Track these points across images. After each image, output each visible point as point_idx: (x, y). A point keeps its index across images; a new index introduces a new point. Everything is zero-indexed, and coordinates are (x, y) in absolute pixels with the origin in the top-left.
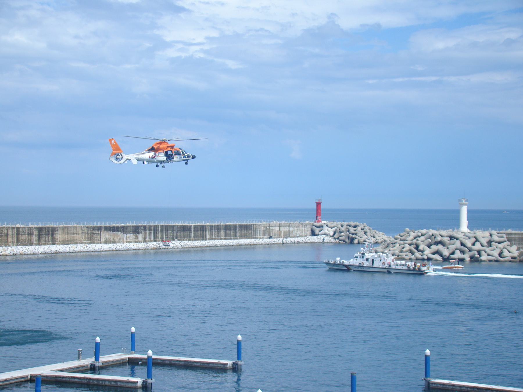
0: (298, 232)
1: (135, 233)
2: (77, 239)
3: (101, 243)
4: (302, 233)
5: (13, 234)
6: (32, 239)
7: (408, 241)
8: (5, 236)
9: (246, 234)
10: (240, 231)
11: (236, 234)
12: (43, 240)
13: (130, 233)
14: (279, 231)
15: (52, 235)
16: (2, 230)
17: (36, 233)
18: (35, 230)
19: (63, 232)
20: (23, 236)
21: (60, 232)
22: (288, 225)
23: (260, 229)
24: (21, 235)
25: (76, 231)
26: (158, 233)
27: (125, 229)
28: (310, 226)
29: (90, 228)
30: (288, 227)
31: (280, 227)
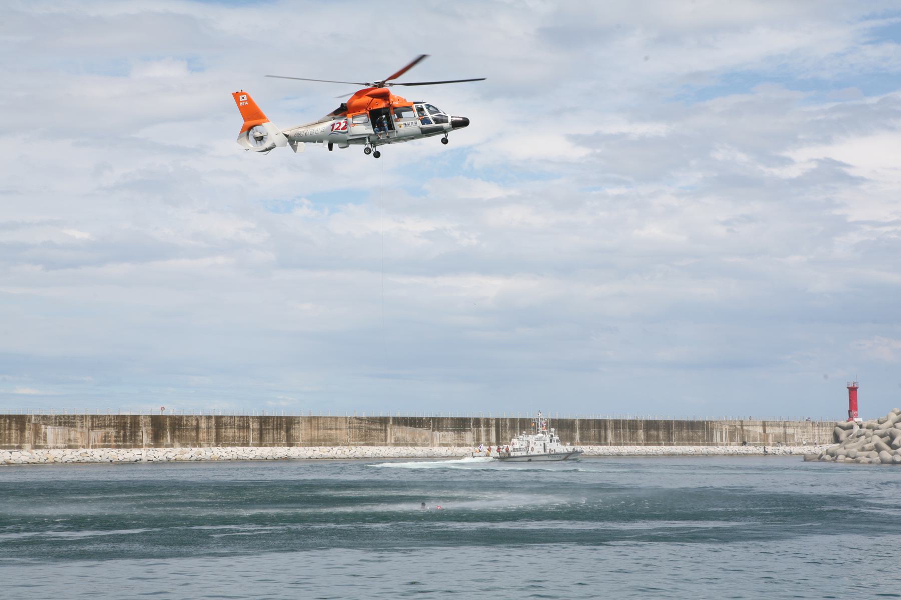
0: (805, 437)
1: (458, 431)
2: (338, 437)
3: (386, 445)
4: (814, 437)
5: (208, 428)
6: (247, 436)
7: (881, 429)
8: (192, 430)
9: (692, 436)
10: (679, 431)
11: (669, 437)
12: (268, 437)
13: (447, 431)
14: (763, 434)
15: (288, 430)
16: (186, 420)
17: (254, 425)
18: (253, 422)
19: (309, 425)
20: (229, 430)
21: (303, 425)
22: (782, 423)
23: (722, 429)
24: (226, 428)
25: (336, 424)
26: (506, 430)
27: (436, 424)
28: (831, 427)
29: (365, 420)
30: (781, 428)
31: (764, 425)
